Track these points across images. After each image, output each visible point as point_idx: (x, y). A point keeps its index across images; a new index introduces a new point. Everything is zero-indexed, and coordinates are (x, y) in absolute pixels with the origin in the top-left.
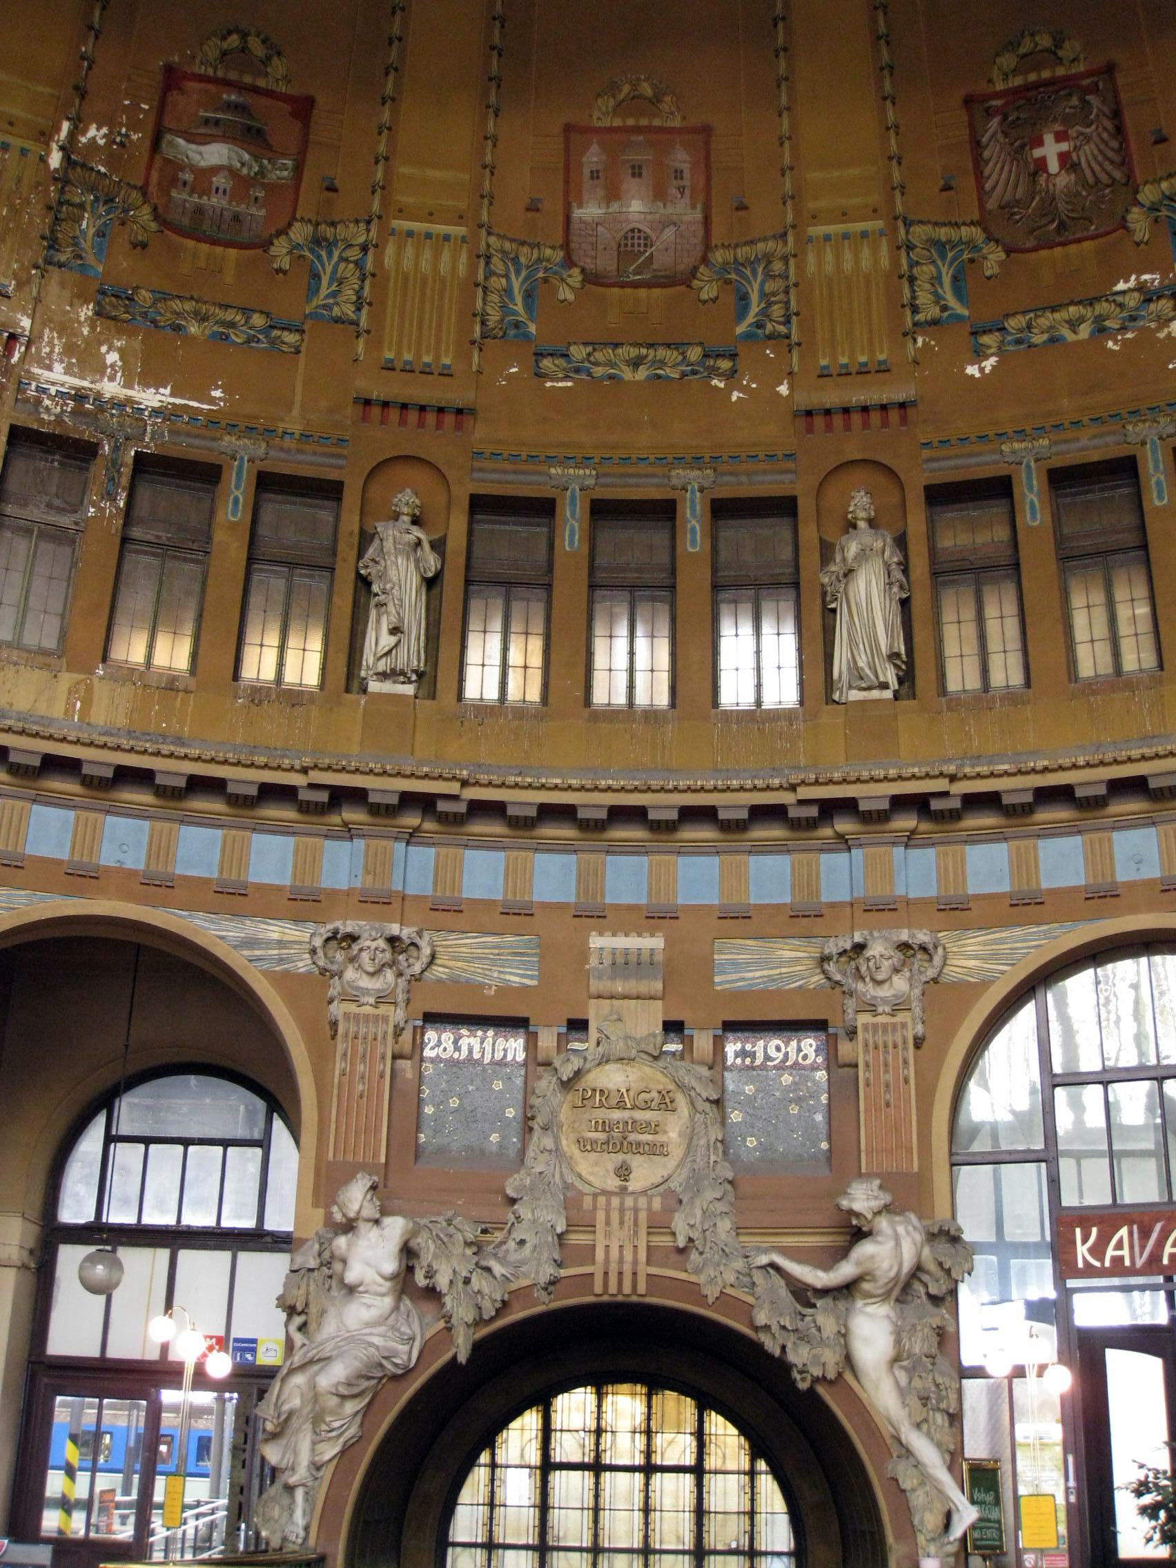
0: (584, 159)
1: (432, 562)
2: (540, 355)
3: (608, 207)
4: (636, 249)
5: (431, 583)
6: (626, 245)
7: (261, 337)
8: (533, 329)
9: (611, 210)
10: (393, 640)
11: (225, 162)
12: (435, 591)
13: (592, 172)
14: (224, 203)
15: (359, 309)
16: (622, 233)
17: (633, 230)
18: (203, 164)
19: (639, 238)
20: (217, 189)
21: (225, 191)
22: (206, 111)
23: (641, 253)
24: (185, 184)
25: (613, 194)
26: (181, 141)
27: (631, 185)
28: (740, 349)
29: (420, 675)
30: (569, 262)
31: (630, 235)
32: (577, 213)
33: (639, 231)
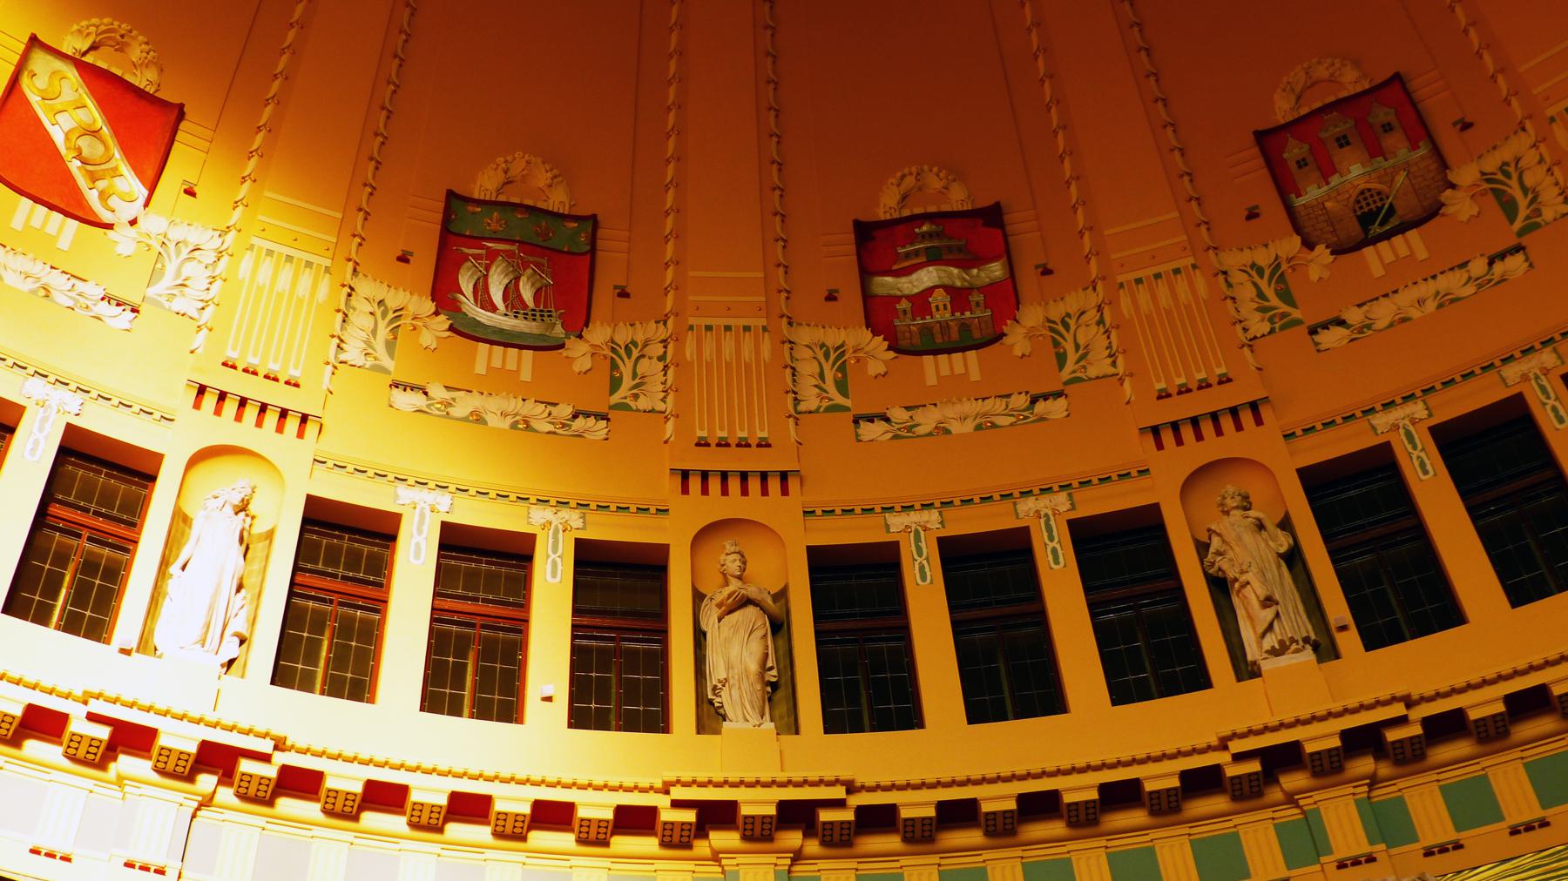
0: (1285, 156)
1: (1283, 542)
2: (1313, 331)
3: (1327, 183)
4: (1373, 206)
5: (1293, 558)
6: (1361, 208)
7: (1026, 414)
8: (1296, 314)
9: (1332, 184)
10: (1269, 614)
11: (937, 282)
12: (1299, 567)
13: (1298, 162)
14: (948, 316)
15: (1114, 364)
16: (1352, 200)
17: (1362, 193)
18: (916, 291)
19: (1372, 196)
20: (937, 306)
21: (945, 305)
22: (903, 247)
23: (1379, 209)
24: (905, 311)
25: (1327, 170)
26: (889, 279)
27: (1340, 156)
28: (1524, 241)
29: (1316, 647)
30: (1309, 245)
31: (1361, 198)
32: (1299, 202)
33: (1369, 190)
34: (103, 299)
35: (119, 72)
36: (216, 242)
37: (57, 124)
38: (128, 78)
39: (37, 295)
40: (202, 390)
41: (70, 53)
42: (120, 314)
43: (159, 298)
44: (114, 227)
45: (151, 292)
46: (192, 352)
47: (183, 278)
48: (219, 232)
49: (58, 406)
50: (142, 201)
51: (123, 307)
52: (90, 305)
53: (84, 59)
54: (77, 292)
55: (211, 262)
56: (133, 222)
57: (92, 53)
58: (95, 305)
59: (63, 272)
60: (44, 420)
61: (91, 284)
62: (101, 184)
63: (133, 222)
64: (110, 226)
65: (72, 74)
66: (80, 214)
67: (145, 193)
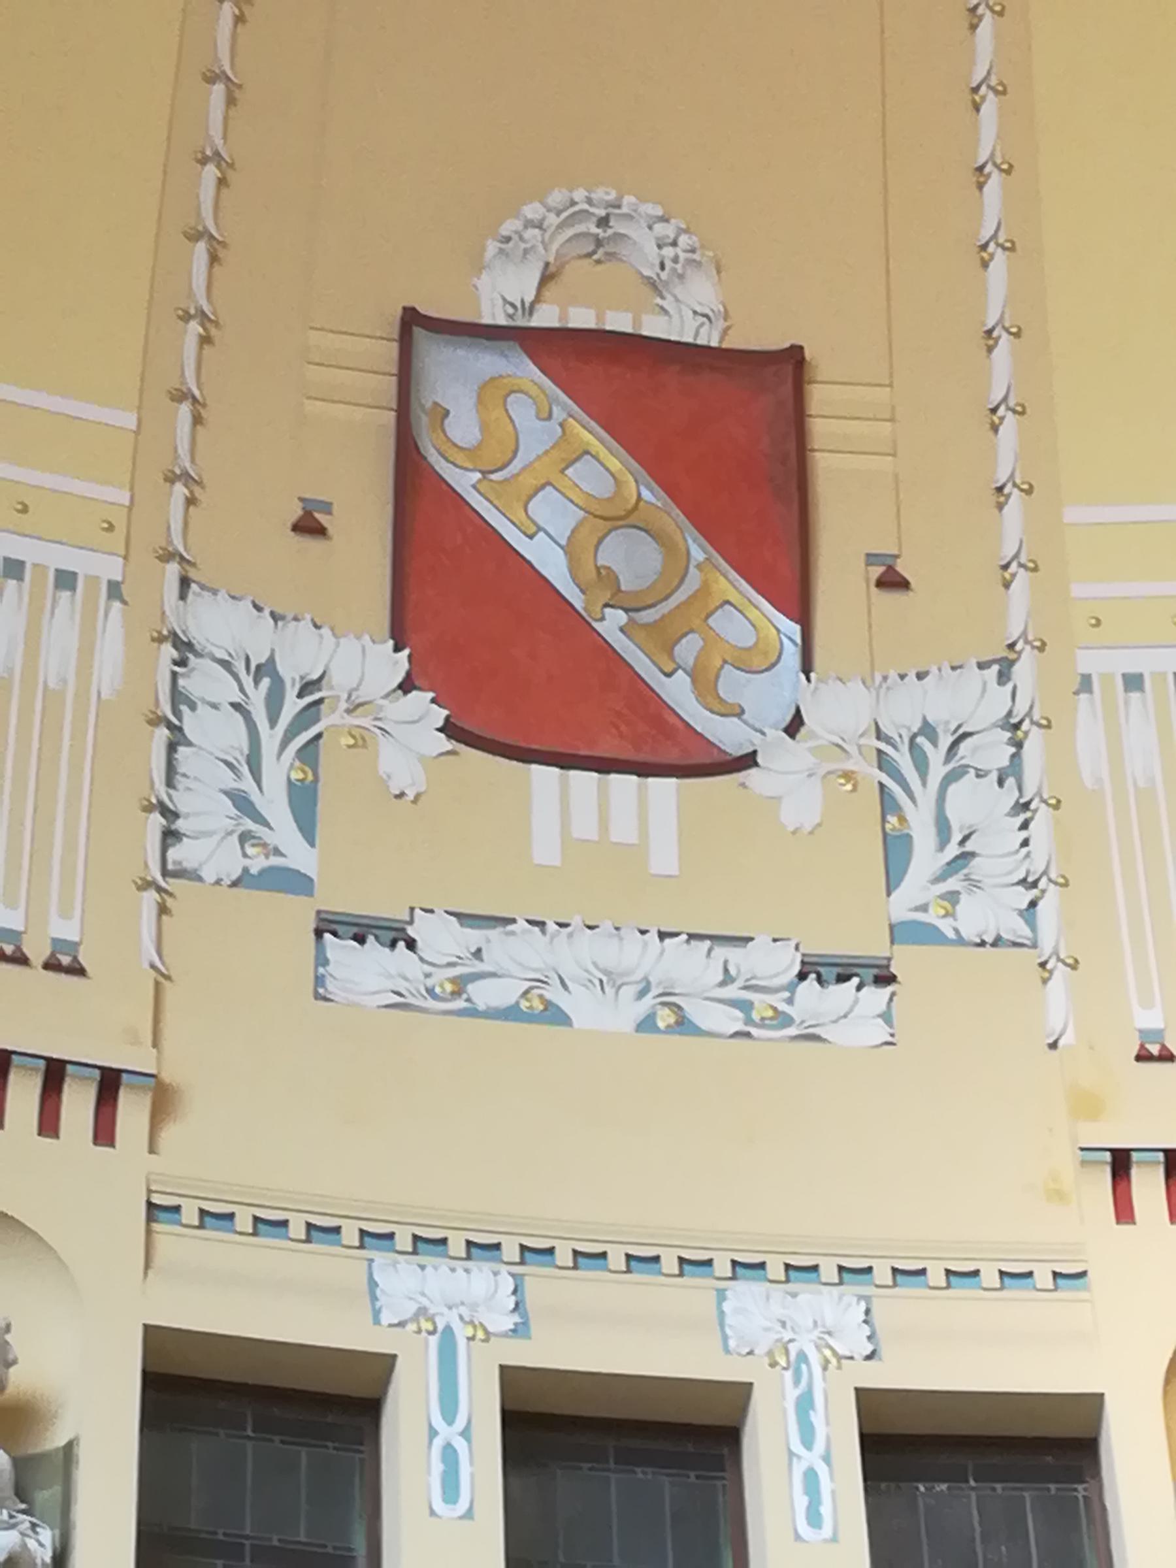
34: (802, 976)
35: (619, 322)
36: (998, 701)
37: (540, 529)
38: (654, 327)
39: (657, 1030)
40: (1121, 1162)
41: (502, 321)
42: (856, 1001)
43: (920, 916)
44: (759, 760)
45: (901, 906)
46: (1053, 1046)
47: (957, 837)
48: (995, 668)
49: (818, 1347)
50: (792, 656)
51: (855, 981)
52: (783, 1007)
53: (537, 321)
54: (740, 983)
55: (1005, 762)
56: (794, 726)
57: (549, 292)
58: (790, 1001)
59: (692, 937)
60: (805, 1404)
61: (762, 940)
62: (688, 649)
63: (794, 726)
64: (748, 761)
65: (527, 371)
66: (672, 756)
67: (794, 629)
